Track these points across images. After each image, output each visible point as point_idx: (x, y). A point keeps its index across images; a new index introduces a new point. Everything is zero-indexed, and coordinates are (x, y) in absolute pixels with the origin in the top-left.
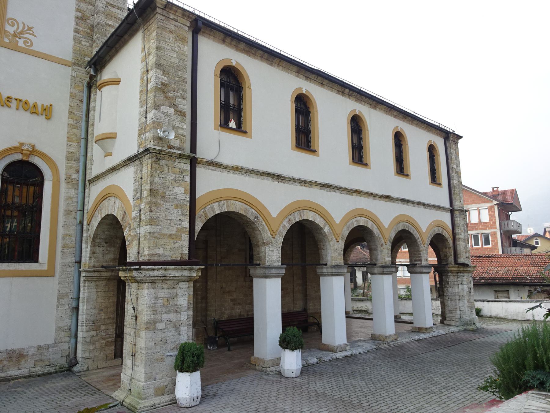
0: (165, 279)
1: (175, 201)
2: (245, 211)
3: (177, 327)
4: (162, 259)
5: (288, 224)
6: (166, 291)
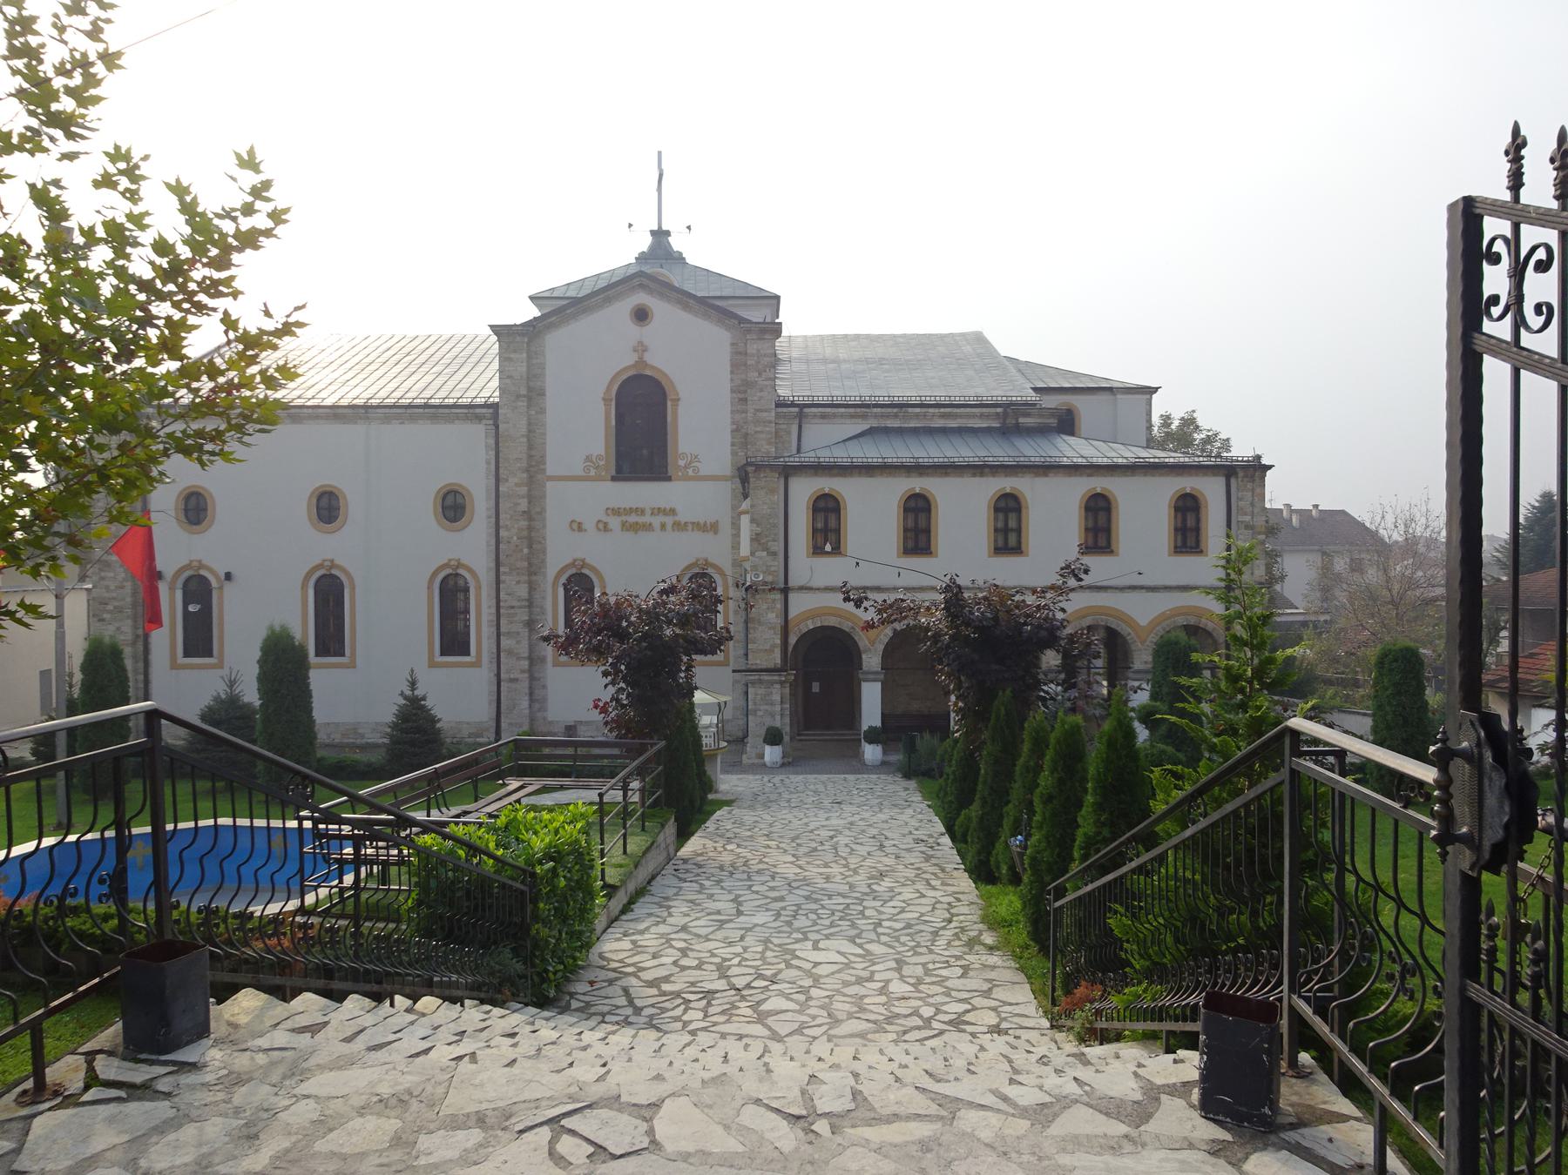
0: (760, 682)
3: (772, 715)
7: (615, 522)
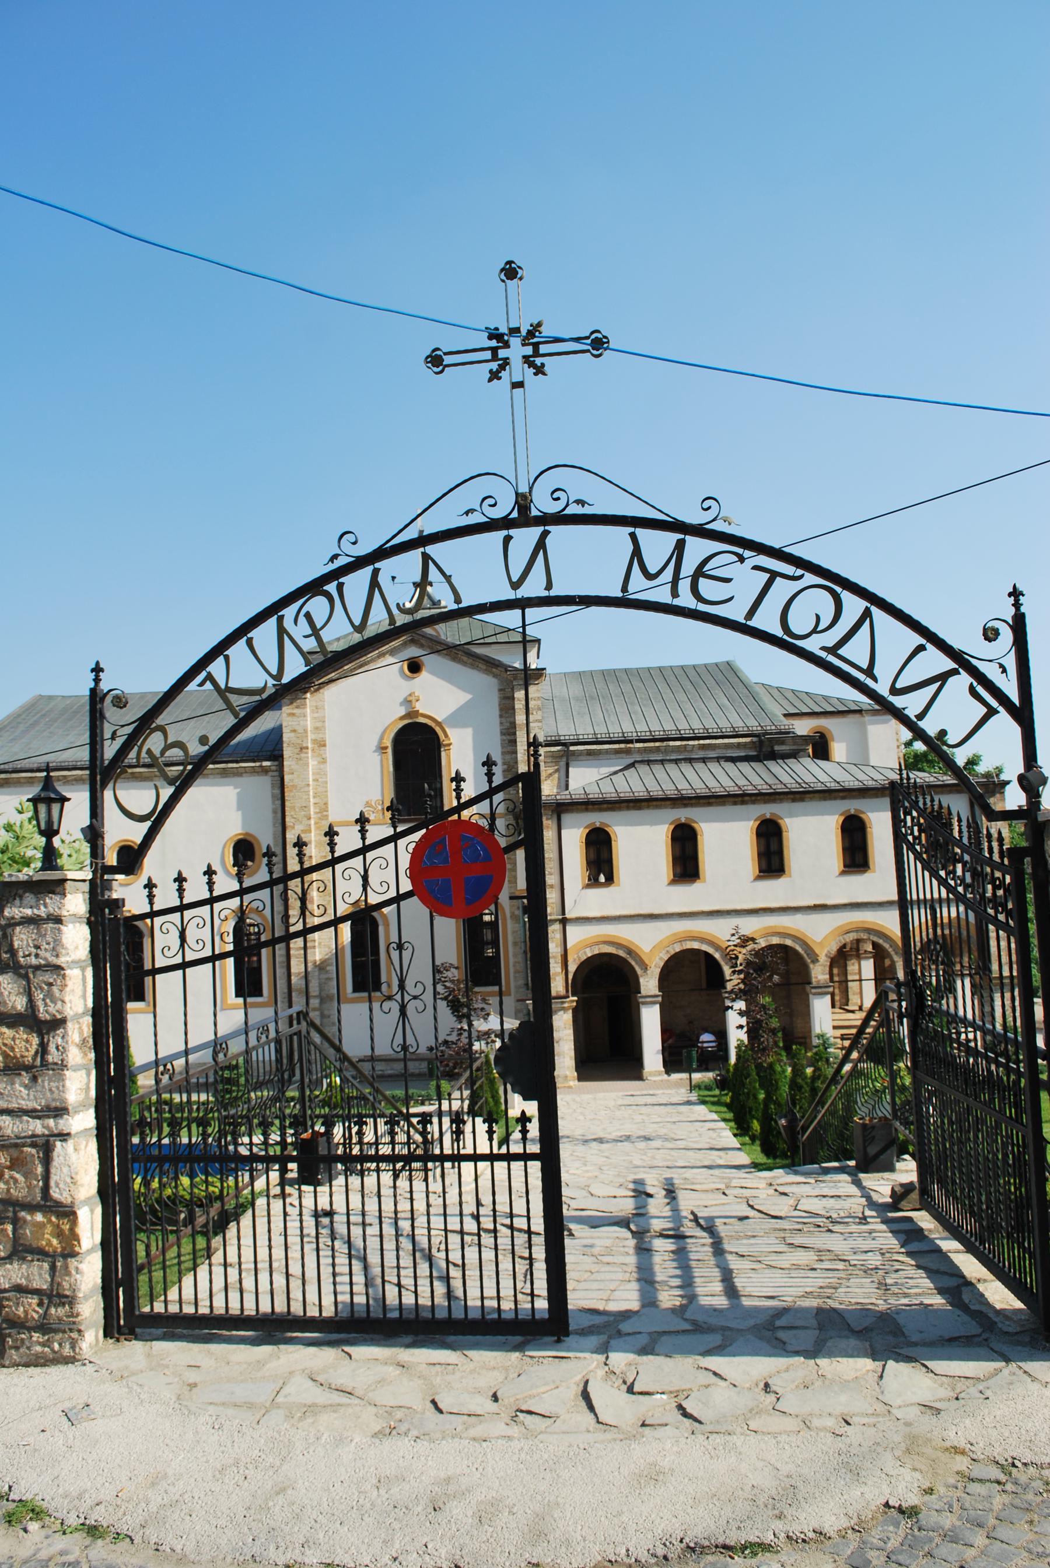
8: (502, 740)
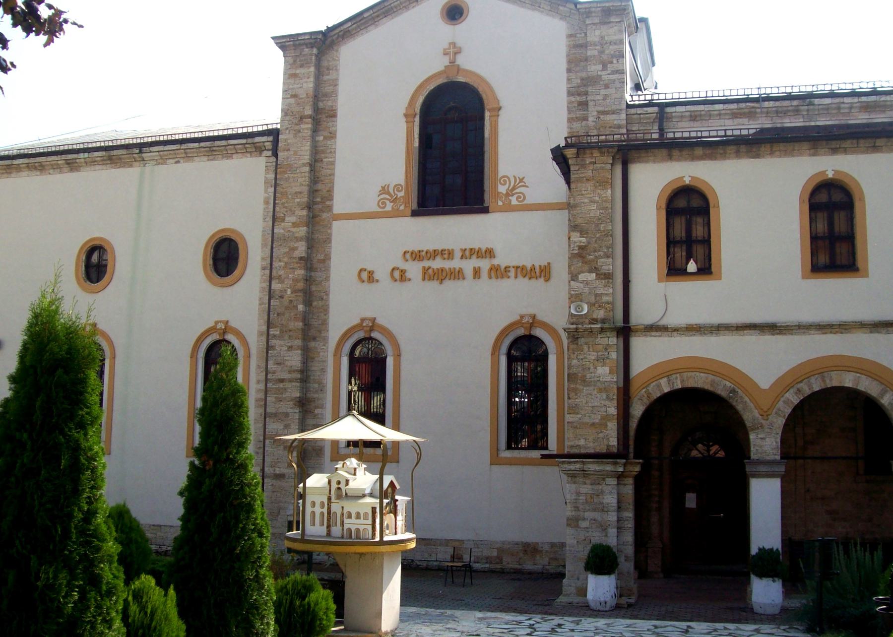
0: (584, 473)
1: (599, 384)
2: (711, 385)
3: (604, 528)
4: (583, 451)
5: (796, 397)
6: (590, 487)
7: (414, 269)
8: (570, 103)
